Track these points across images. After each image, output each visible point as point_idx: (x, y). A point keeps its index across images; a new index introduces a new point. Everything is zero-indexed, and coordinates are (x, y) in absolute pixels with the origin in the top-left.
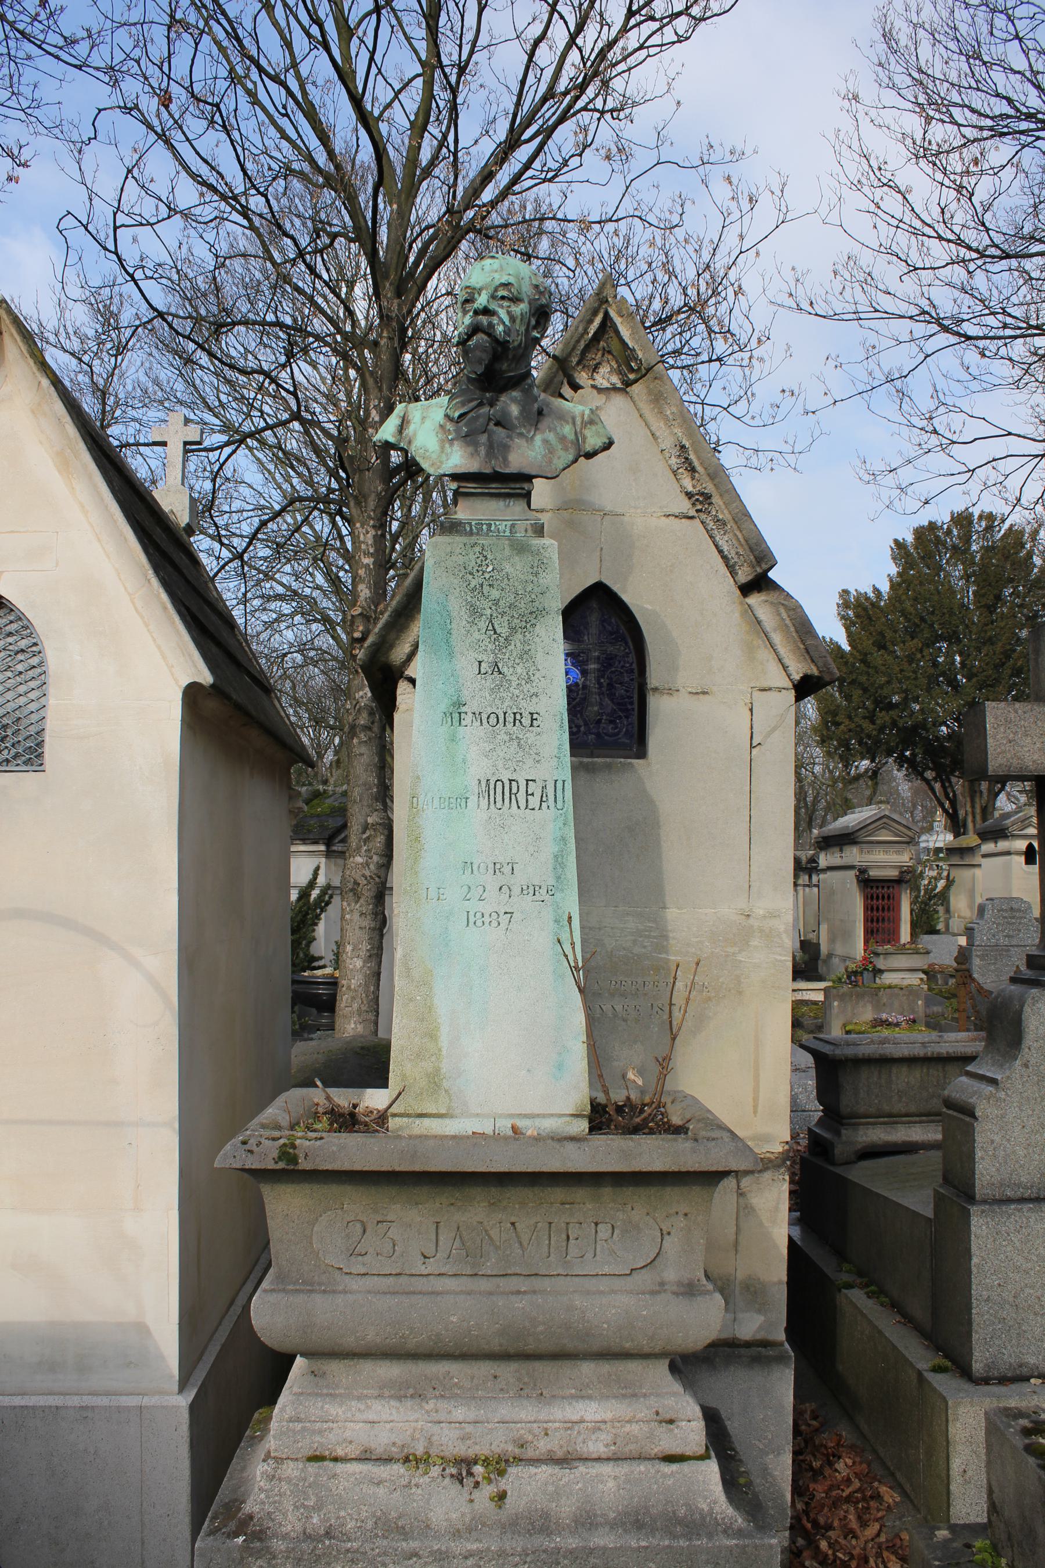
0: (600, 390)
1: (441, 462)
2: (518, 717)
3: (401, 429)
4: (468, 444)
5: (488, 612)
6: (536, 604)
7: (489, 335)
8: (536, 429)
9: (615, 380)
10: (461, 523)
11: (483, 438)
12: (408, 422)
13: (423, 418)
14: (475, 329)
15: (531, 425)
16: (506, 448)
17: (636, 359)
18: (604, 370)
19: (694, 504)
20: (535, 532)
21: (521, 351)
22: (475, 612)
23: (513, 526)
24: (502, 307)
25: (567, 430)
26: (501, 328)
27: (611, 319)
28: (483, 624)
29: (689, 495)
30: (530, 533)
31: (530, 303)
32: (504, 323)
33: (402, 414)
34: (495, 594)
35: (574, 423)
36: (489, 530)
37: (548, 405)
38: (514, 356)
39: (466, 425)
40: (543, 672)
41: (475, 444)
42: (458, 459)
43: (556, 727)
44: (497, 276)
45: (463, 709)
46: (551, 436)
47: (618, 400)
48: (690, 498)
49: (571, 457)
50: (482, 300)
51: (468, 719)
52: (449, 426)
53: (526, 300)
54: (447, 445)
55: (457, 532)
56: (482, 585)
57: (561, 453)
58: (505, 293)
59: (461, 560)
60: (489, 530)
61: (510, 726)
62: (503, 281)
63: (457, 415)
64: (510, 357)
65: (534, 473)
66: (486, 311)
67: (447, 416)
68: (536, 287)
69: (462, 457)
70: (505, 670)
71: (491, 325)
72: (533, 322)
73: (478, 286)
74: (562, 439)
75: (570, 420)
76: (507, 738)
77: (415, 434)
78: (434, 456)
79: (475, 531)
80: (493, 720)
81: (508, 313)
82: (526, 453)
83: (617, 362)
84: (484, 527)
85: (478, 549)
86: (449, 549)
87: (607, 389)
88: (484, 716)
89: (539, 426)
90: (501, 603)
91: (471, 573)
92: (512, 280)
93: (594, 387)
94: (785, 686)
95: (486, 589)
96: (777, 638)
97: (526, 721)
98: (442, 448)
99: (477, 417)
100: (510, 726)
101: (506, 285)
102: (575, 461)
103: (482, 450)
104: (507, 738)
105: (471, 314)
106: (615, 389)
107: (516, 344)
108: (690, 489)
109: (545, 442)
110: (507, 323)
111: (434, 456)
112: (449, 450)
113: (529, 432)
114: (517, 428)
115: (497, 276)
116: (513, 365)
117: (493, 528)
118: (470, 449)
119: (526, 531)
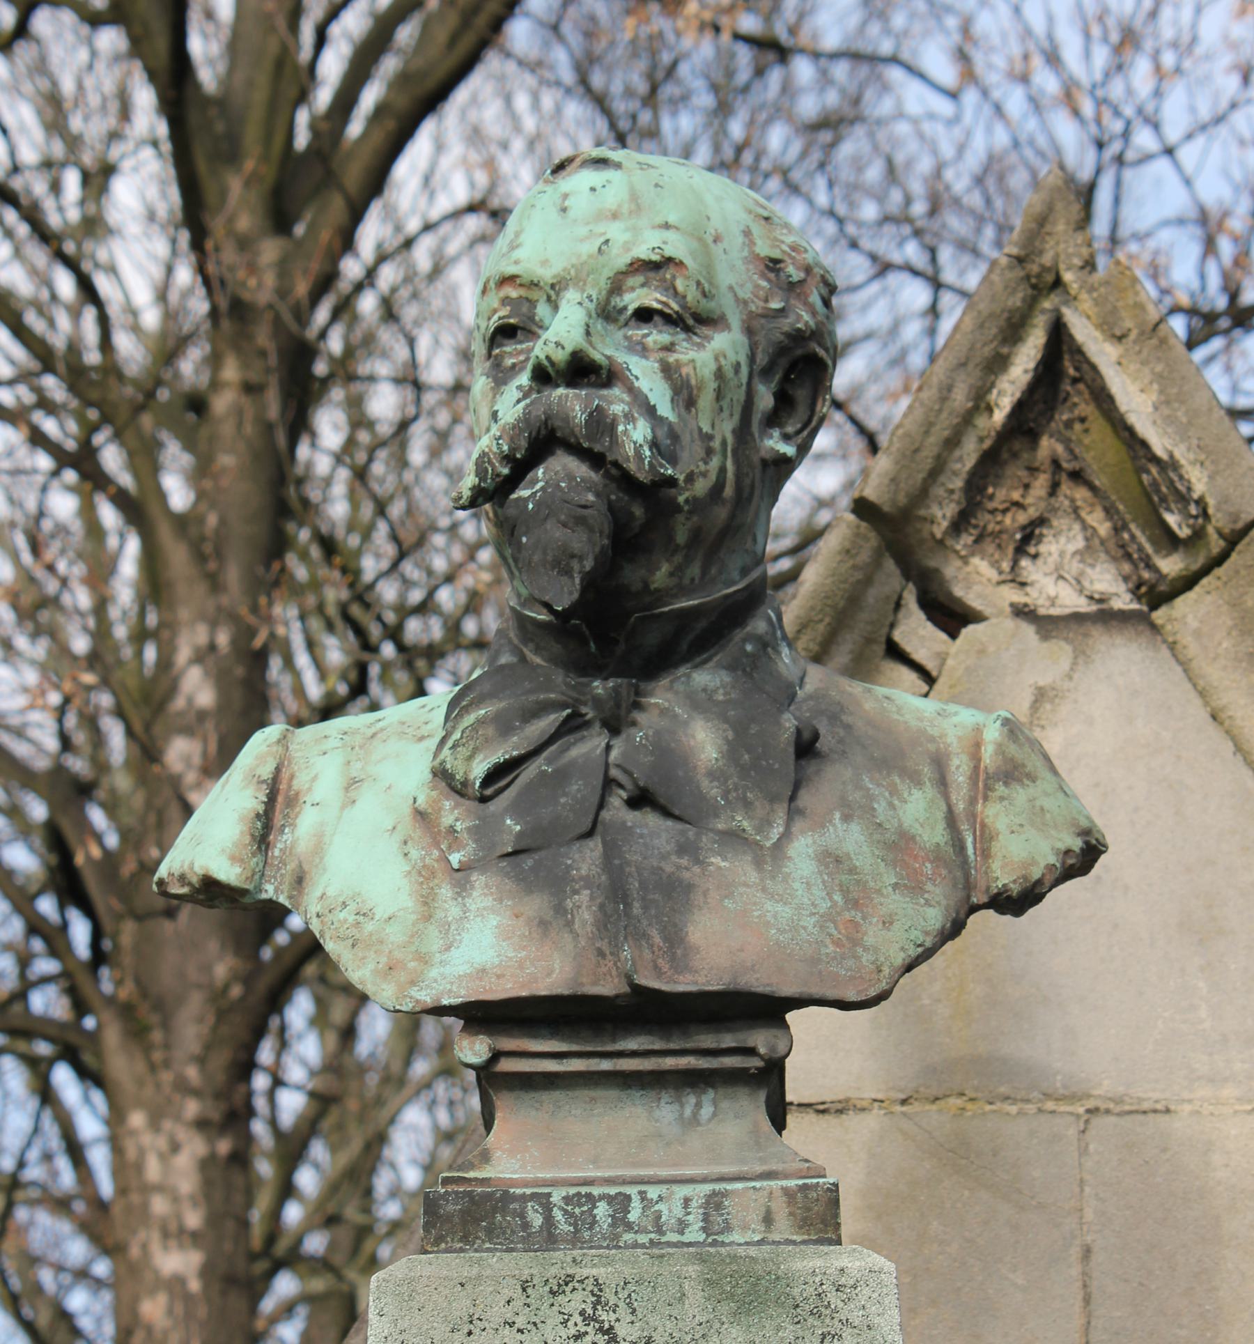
0: (1046, 624)
1: (424, 959)
4: (527, 883)
7: (596, 460)
8: (794, 812)
9: (1108, 581)
10: (507, 1197)
11: (586, 859)
12: (293, 801)
13: (352, 784)
14: (541, 441)
15: (773, 799)
16: (674, 894)
17: (1183, 499)
18: (1062, 544)
20: (804, 1223)
21: (721, 514)
23: (714, 1203)
24: (642, 350)
25: (917, 810)
26: (638, 433)
27: (1078, 351)
30: (783, 1228)
31: (749, 331)
32: (651, 411)
33: (266, 771)
35: (942, 783)
37: (835, 714)
38: (696, 536)
39: (516, 810)
41: (557, 885)
42: (487, 945)
44: (616, 232)
46: (851, 839)
47: (1123, 660)
49: (935, 918)
50: (564, 329)
52: (452, 814)
53: (735, 320)
54: (445, 892)
55: (490, 1233)
57: (895, 902)
58: (651, 298)
62: (643, 251)
63: (479, 769)
64: (681, 537)
65: (788, 989)
66: (581, 371)
67: (442, 774)
68: (773, 265)
69: (504, 934)
71: (601, 423)
72: (765, 399)
73: (547, 275)
74: (899, 846)
75: (927, 771)
77: (319, 849)
78: (395, 934)
79: (564, 1227)
81: (667, 370)
82: (751, 912)
83: (1109, 511)
84: (602, 1210)
85: (577, 1301)
86: (461, 1307)
87: (1078, 618)
89: (806, 799)
92: (676, 246)
93: (1023, 612)
98: (427, 902)
99: (561, 777)
102: (955, 929)
103: (584, 908)
105: (524, 379)
106: (1107, 616)
107: (701, 487)
109: (832, 860)
110: (665, 409)
111: (395, 934)
112: (454, 911)
113: (766, 823)
114: (715, 812)
115: (616, 232)
116: (695, 570)
117: (633, 1216)
118: (537, 904)
119: (768, 1220)
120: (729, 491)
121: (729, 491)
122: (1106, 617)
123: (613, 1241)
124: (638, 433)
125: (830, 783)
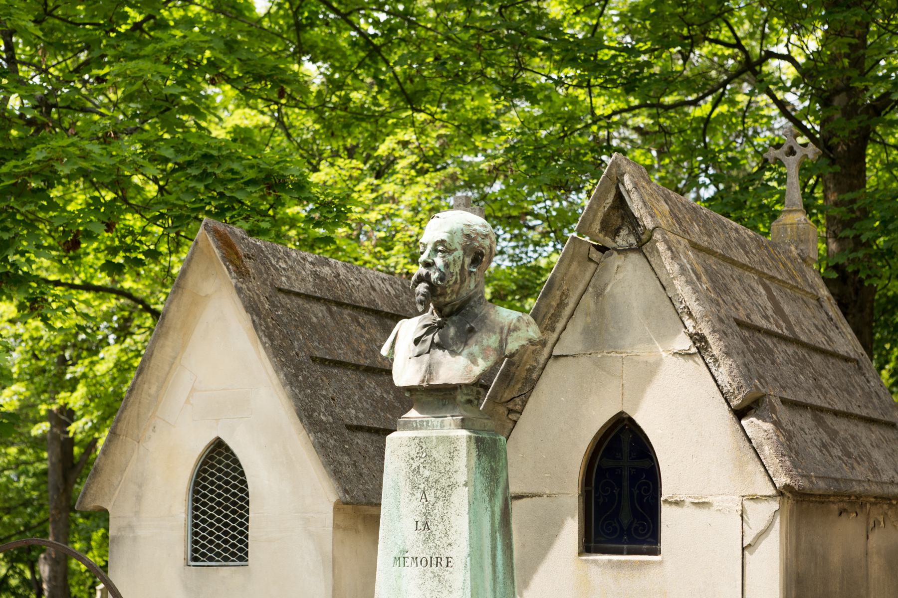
2: (439, 560)
3: (393, 346)
5: (422, 486)
6: (452, 480)
9: (632, 240)
11: (426, 357)
18: (624, 232)
19: (695, 343)
21: (458, 286)
22: (415, 487)
23: (442, 422)
25: (493, 341)
28: (419, 495)
29: (691, 336)
30: (453, 426)
31: (464, 249)
34: (427, 473)
36: (427, 425)
40: (455, 528)
41: (421, 363)
43: (462, 566)
45: (406, 555)
47: (634, 257)
48: (691, 338)
51: (409, 561)
53: (459, 247)
56: (419, 467)
58: (440, 248)
59: (407, 449)
60: (427, 425)
61: (434, 566)
62: (439, 239)
68: (468, 236)
70: (431, 527)
71: (428, 275)
75: (498, 331)
76: (432, 575)
80: (424, 563)
85: (417, 441)
88: (419, 560)
89: (470, 342)
90: (431, 479)
91: (413, 459)
94: (770, 493)
95: (421, 469)
96: (767, 451)
97: (444, 563)
100: (434, 566)
101: (442, 242)
104: (432, 575)
108: (691, 330)
118: (417, 366)
120: (459, 281)
121: (459, 281)
122: (630, 249)
123: (426, 429)
124: (434, 276)
125: (476, 337)
